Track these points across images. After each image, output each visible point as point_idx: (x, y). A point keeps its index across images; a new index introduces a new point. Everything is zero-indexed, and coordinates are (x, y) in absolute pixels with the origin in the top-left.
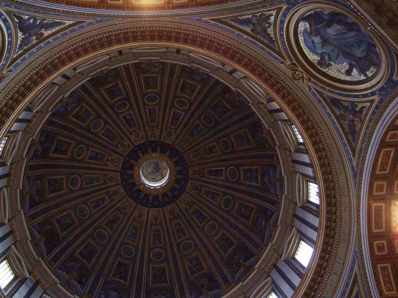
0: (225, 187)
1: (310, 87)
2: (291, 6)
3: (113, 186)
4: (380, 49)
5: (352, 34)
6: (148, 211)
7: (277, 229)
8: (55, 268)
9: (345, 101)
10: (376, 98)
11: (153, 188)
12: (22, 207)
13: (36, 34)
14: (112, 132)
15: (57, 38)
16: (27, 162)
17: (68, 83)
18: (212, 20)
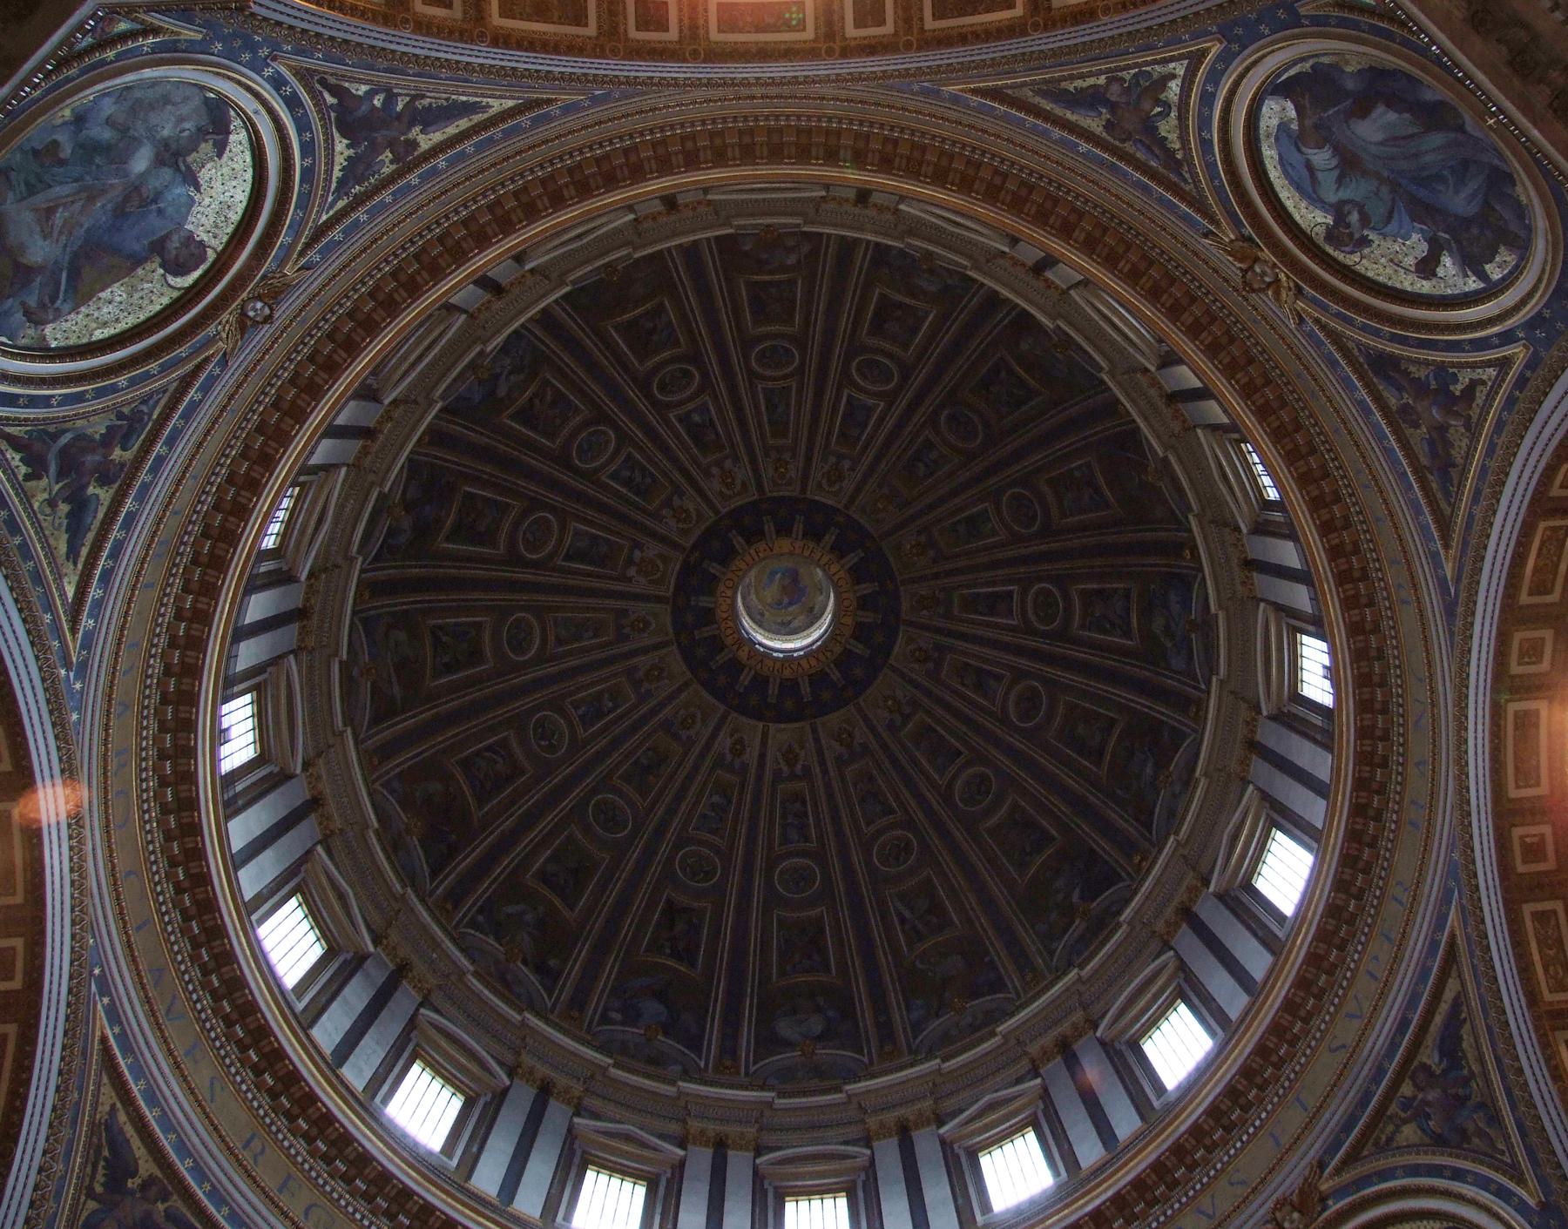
0: (1020, 651)
1: (1300, 317)
2: (1235, 47)
3: (645, 651)
4: (1527, 192)
5: (1437, 139)
6: (765, 735)
7: (1193, 792)
8: (459, 923)
9: (1417, 362)
10: (1518, 352)
11: (781, 655)
12: (349, 720)
13: (391, 145)
14: (643, 470)
15: (462, 156)
16: (362, 571)
17: (497, 305)
18: (975, 92)
